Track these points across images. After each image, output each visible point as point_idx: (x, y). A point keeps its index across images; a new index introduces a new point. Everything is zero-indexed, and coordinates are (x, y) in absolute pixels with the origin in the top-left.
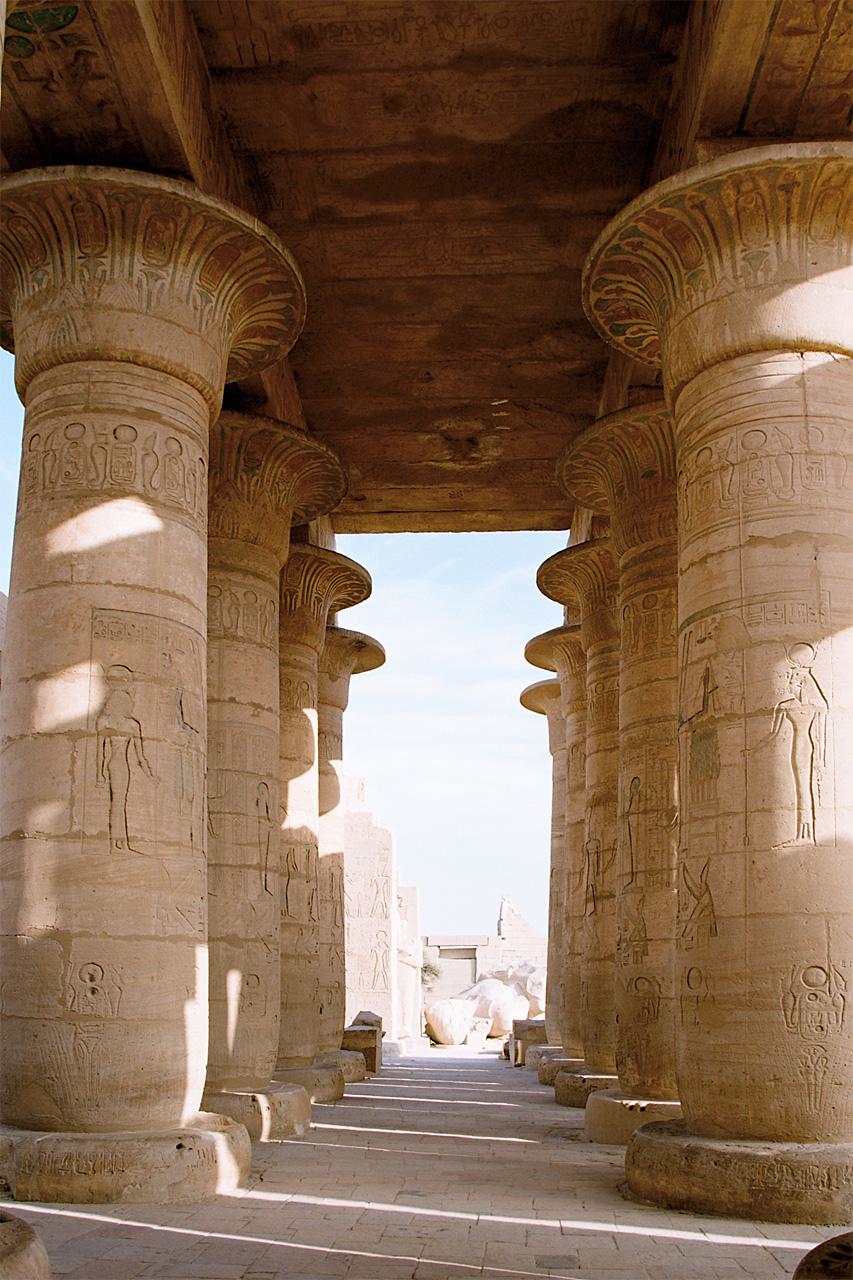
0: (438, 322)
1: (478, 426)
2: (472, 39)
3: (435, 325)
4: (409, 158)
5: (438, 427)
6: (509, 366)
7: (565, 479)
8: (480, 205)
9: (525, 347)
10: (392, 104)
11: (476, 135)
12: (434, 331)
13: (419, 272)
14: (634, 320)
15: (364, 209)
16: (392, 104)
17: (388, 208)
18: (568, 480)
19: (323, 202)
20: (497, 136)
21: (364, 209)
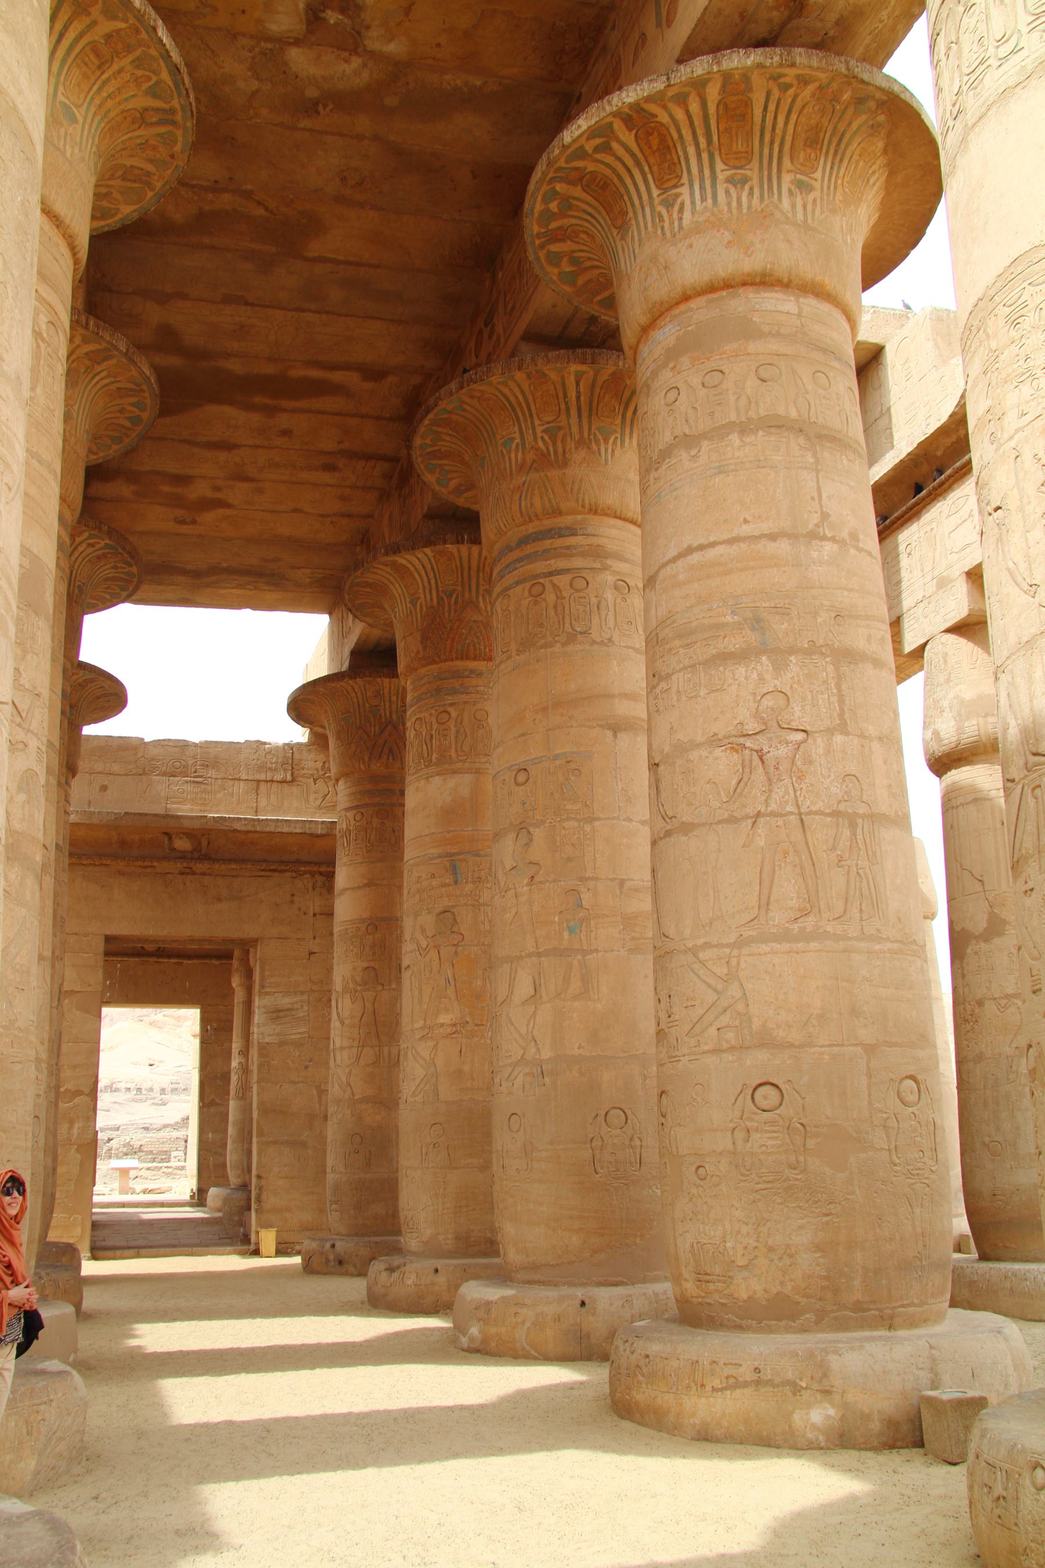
0: (306, 259)
1: (298, 59)
2: (223, 456)
3: (311, 255)
4: (285, 403)
5: (365, 65)
6: (231, 179)
7: (147, 395)
8: (235, 366)
9: (207, 208)
10: (286, 433)
11: (229, 411)
12: (315, 248)
13: (309, 316)
14: (100, 553)
15: (336, 377)
16: (286, 433)
17: (315, 373)
18: (143, 391)
19: (369, 385)
20: (212, 409)
21: (336, 377)
